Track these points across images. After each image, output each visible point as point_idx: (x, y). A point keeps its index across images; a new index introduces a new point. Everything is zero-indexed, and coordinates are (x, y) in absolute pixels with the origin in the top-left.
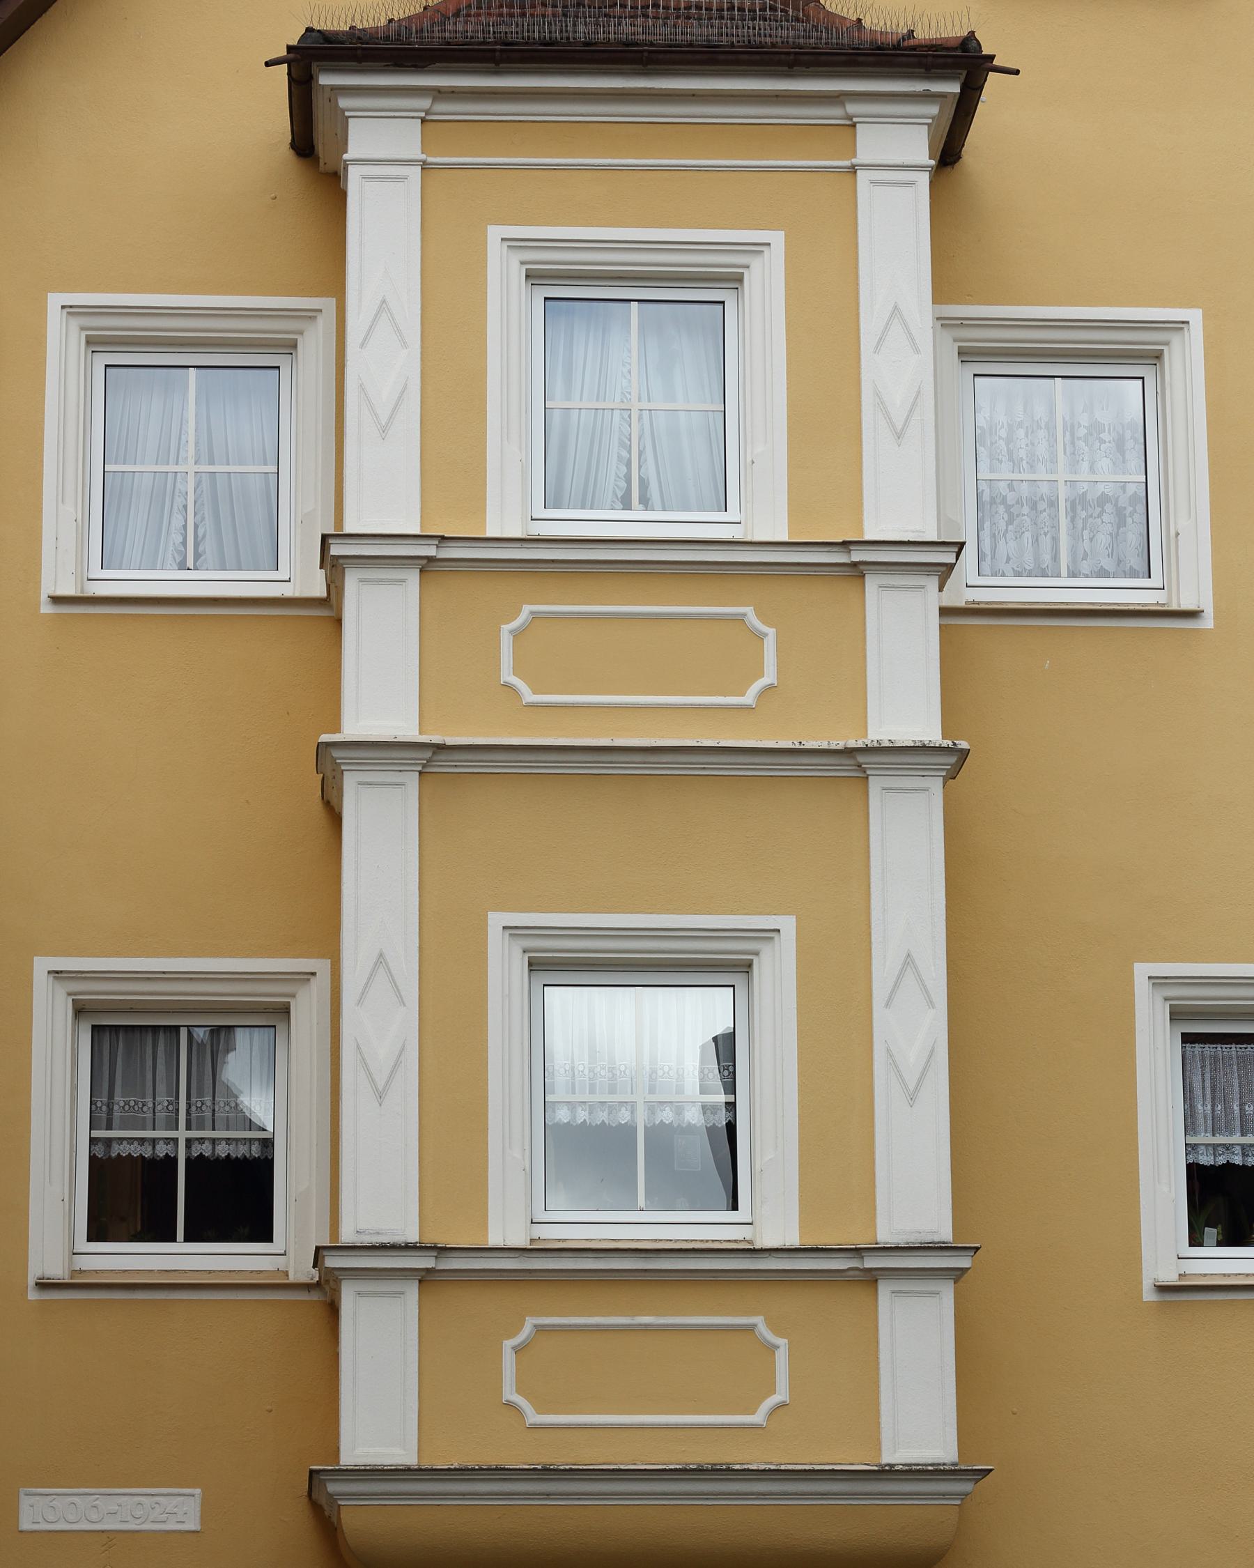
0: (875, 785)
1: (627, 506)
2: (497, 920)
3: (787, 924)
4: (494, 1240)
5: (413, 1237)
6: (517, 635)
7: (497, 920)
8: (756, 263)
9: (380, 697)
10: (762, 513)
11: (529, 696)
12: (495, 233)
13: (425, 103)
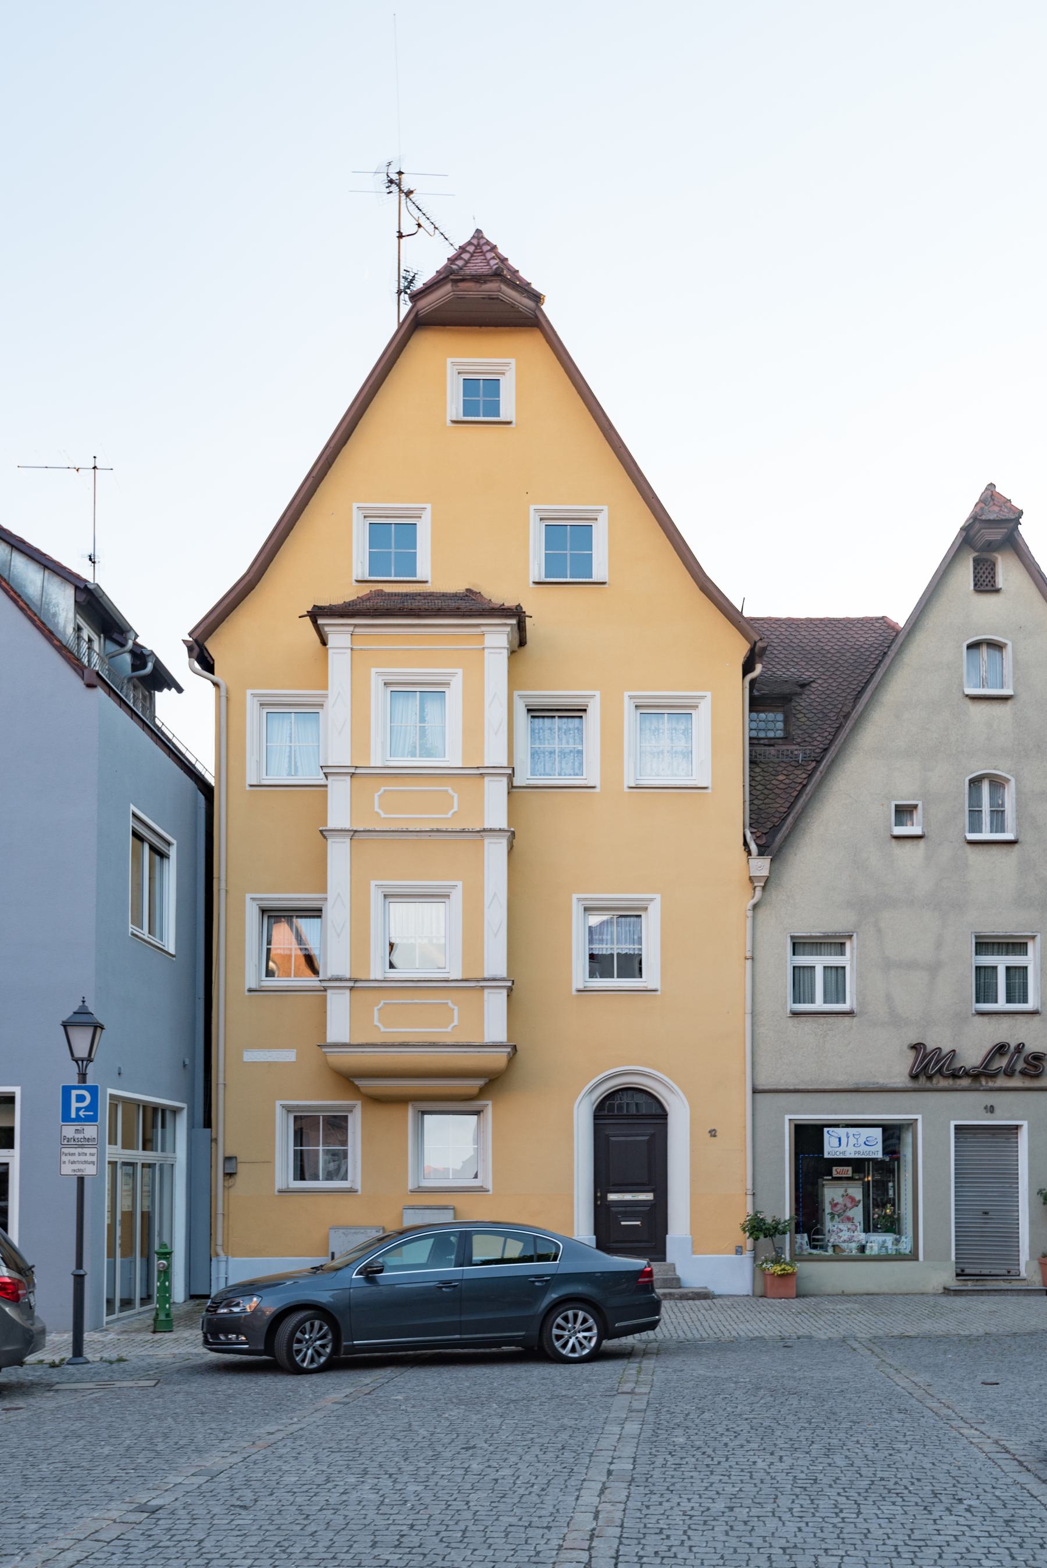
0: (486, 841)
2: (373, 883)
3: (460, 884)
4: (372, 978)
5: (348, 976)
6: (380, 796)
7: (373, 883)
9: (339, 816)
10: (453, 758)
11: (383, 815)
12: (374, 670)
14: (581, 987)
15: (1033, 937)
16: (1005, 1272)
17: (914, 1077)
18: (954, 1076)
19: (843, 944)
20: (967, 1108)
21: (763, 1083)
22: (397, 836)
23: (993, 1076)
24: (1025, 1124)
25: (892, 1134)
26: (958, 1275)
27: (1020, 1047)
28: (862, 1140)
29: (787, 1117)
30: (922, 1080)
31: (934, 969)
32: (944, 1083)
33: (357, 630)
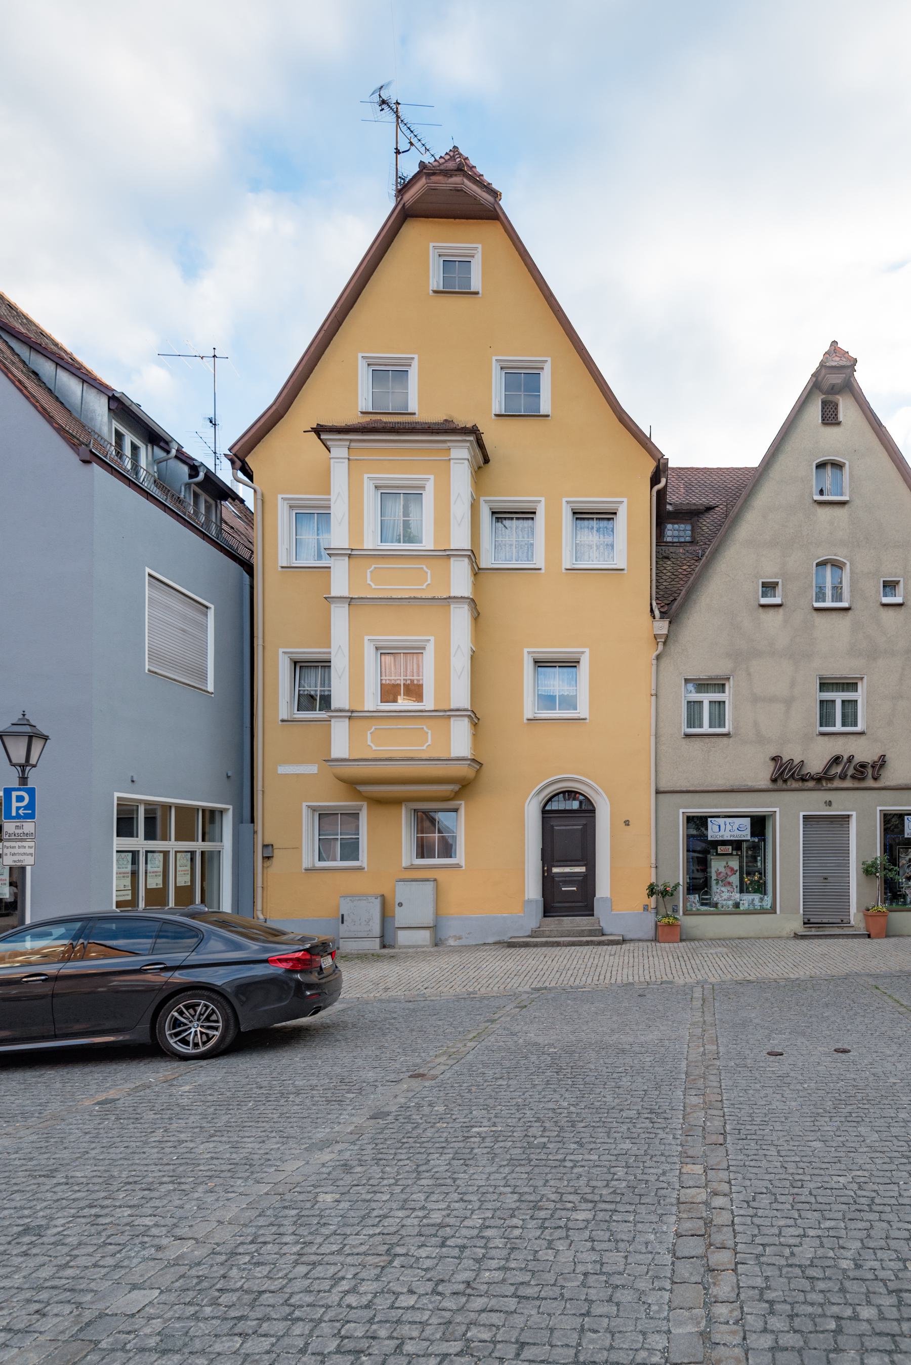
1: (400, 542)
6: (371, 572)
8: (428, 483)
13: (348, 443)
14: (531, 717)
15: (862, 679)
16: (839, 921)
17: (774, 781)
18: (803, 780)
19: (724, 685)
20: (813, 802)
21: (663, 786)
22: (383, 602)
23: (831, 779)
24: (854, 813)
25: (759, 824)
26: (805, 923)
27: (851, 759)
28: (735, 827)
29: (681, 811)
30: (780, 782)
31: (788, 702)
32: (795, 785)
33: (353, 444)
